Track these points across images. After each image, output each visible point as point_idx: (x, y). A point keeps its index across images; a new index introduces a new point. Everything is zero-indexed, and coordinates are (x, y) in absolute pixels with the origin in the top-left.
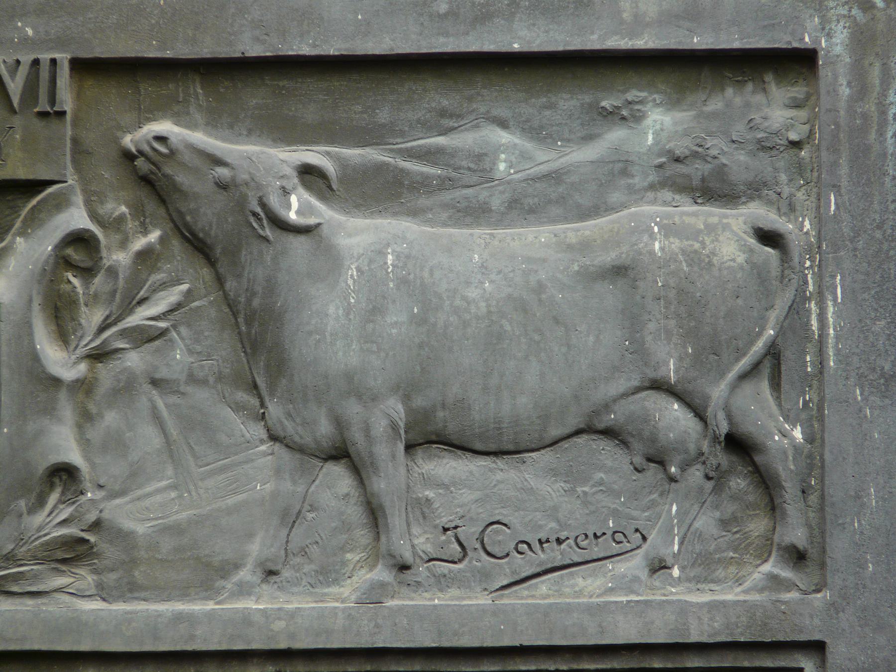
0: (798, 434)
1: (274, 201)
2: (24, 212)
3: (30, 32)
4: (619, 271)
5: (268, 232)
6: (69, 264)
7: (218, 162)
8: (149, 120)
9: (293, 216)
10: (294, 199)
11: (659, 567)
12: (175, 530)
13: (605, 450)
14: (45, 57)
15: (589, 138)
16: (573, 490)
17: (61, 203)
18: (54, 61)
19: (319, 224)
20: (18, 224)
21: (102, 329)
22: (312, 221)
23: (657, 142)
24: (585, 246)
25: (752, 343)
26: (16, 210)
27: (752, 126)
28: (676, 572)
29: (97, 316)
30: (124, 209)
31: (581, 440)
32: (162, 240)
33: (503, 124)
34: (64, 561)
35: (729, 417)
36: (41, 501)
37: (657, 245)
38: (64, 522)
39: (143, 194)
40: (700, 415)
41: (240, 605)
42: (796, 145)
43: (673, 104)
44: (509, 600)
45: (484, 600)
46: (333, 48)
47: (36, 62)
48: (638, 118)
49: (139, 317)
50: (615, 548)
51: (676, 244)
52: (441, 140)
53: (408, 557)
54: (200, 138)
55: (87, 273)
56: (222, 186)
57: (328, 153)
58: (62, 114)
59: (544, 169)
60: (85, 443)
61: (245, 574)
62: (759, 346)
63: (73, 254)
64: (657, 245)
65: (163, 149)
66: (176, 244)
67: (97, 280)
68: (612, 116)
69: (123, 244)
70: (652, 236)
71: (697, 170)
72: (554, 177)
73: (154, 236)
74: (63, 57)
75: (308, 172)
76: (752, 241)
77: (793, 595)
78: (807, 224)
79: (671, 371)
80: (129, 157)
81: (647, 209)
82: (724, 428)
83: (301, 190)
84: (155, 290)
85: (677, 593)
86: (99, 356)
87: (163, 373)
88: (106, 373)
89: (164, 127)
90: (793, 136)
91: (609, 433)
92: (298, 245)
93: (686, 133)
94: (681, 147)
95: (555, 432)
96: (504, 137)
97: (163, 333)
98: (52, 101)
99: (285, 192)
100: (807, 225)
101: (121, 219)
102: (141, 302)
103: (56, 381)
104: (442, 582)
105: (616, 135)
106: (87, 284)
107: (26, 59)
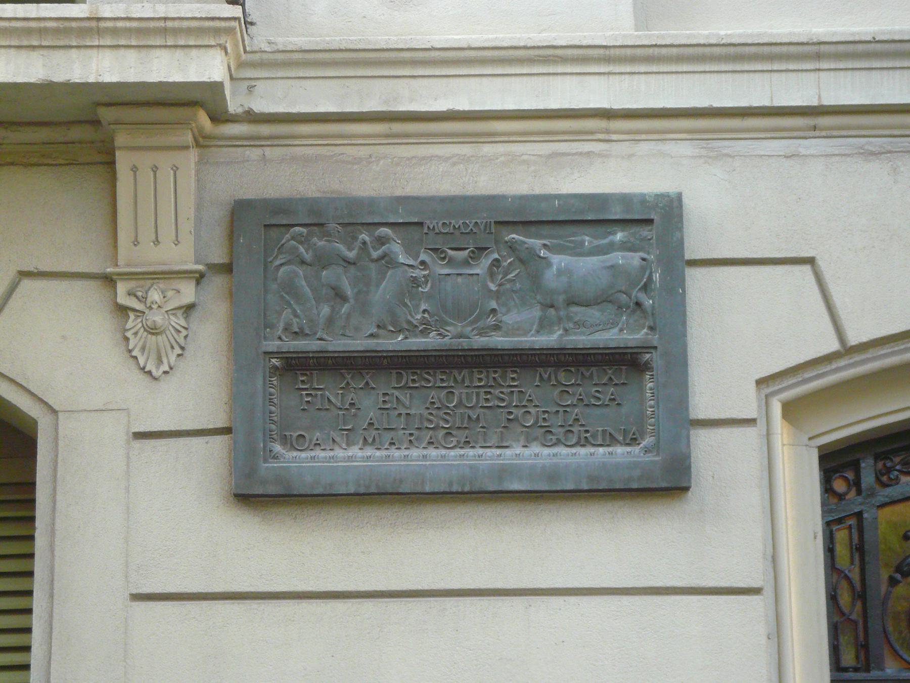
0: (651, 302)
1: (538, 252)
2: (485, 253)
3: (485, 215)
4: (612, 266)
5: (537, 258)
6: (494, 265)
7: (525, 243)
8: (511, 234)
9: (542, 255)
10: (542, 251)
11: (621, 330)
12: (517, 322)
13: (610, 306)
14: (489, 221)
15: (605, 238)
16: (603, 314)
17: (492, 252)
18: (490, 222)
19: (547, 257)
20: (483, 256)
21: (501, 279)
22: (546, 256)
23: (620, 239)
24: (603, 261)
25: (640, 282)
26: (483, 253)
27: (641, 235)
28: (625, 332)
29: (500, 277)
30: (505, 253)
31: (605, 303)
32: (514, 260)
33: (587, 235)
34: (495, 329)
35: (636, 298)
36: (489, 316)
37: (620, 261)
38: (494, 321)
39: (510, 250)
40: (630, 298)
41: (532, 339)
42: (650, 239)
43: (622, 231)
44: (590, 337)
45: (584, 338)
46: (550, 219)
47: (487, 222)
48: (616, 234)
49: (510, 276)
50: (612, 326)
51: (624, 261)
52: (573, 238)
53: (568, 328)
54: (521, 238)
55: (498, 267)
56: (527, 248)
57: (549, 241)
58: (492, 233)
59: (595, 245)
60: (497, 303)
61: (533, 332)
62: (642, 283)
63: (495, 263)
64: (620, 261)
65: (514, 241)
66: (517, 262)
67: (500, 269)
68: (610, 233)
69: (506, 261)
70: (619, 259)
71: (629, 245)
72: (598, 246)
73: (512, 259)
74: (493, 221)
75: (545, 245)
76: (641, 260)
77: (650, 336)
78: (652, 257)
79: (623, 288)
80: (506, 242)
81: (618, 253)
82: (635, 301)
83: (544, 250)
84: (512, 271)
85: (625, 336)
86: (500, 285)
87: (514, 289)
88: (502, 288)
89: (513, 236)
90: (649, 238)
91: (610, 302)
92: (544, 261)
93: (625, 237)
94: (625, 240)
95: (599, 301)
96: (587, 238)
97: (514, 280)
98: (490, 231)
99: (540, 250)
100: (652, 257)
101: (505, 256)
102: (510, 273)
103: (491, 291)
104: (575, 334)
105: (611, 237)
106: (498, 270)
107: (485, 221)
